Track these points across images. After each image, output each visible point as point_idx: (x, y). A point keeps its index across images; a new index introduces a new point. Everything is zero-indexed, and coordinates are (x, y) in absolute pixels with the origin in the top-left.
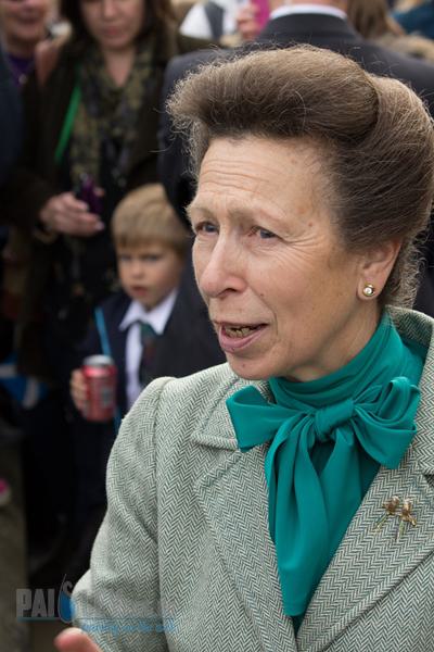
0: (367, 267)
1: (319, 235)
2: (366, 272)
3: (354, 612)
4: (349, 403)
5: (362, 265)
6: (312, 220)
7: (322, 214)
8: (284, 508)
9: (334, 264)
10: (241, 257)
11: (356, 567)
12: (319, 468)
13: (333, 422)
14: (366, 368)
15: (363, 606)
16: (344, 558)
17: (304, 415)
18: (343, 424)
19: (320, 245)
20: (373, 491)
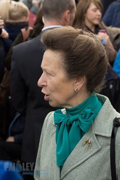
0: (76, 83)
1: (61, 75)
2: (75, 84)
3: (73, 167)
4: (78, 115)
5: (74, 83)
6: (59, 70)
7: (62, 69)
8: (59, 140)
9: (63, 81)
10: (47, 78)
11: (76, 156)
12: (68, 131)
13: (73, 119)
14: (83, 107)
15: (76, 165)
16: (73, 153)
17: (68, 117)
18: (77, 120)
19: (60, 77)
20: (83, 137)
